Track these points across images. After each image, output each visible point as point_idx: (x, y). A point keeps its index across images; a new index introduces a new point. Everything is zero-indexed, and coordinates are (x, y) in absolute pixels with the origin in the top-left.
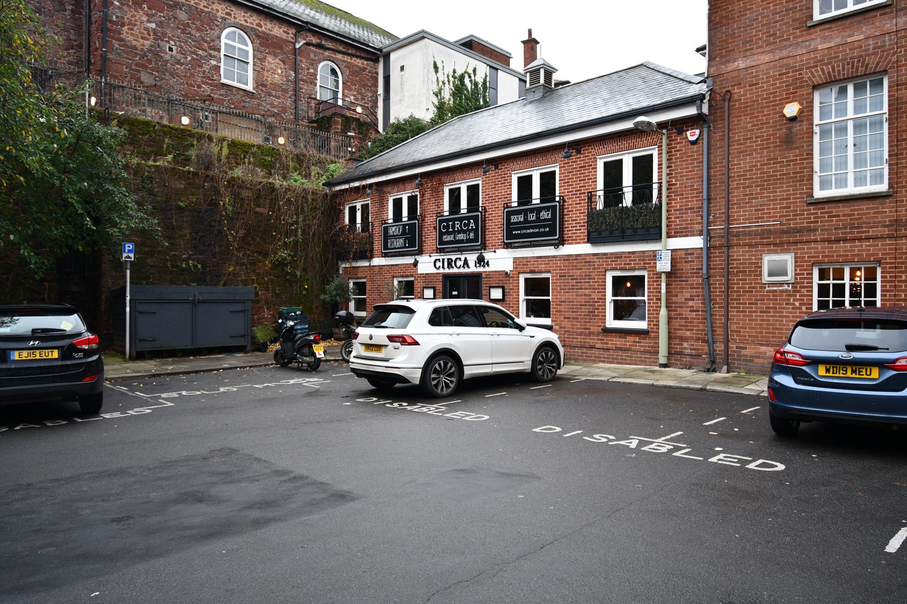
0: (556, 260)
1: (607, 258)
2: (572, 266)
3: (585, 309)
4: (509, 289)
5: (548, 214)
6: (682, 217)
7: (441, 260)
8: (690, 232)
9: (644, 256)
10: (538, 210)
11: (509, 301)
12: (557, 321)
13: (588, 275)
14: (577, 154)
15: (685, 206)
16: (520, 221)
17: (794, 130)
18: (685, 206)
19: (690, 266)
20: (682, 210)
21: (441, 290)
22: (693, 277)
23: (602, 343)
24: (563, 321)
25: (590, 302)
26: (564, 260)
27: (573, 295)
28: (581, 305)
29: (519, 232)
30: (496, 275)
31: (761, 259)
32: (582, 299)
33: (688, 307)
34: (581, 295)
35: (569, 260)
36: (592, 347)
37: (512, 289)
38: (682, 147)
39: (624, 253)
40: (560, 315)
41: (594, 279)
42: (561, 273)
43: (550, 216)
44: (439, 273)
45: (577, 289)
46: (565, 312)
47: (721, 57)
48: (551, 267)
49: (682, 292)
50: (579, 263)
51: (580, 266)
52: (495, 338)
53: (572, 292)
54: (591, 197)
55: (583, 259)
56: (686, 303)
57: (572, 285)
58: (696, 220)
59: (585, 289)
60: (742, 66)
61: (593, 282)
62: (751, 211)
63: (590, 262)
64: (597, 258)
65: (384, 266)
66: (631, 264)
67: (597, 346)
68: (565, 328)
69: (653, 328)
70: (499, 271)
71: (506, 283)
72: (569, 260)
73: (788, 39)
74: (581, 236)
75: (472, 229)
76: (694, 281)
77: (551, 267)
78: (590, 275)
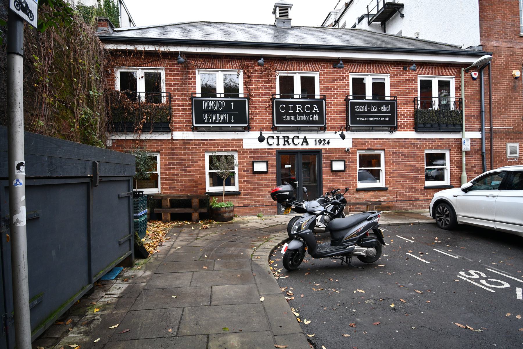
0: (389, 142)
1: (426, 141)
2: (401, 146)
3: (411, 175)
4: (349, 162)
5: (388, 108)
6: (469, 120)
7: (275, 137)
8: (473, 129)
9: (449, 141)
10: (369, 104)
11: (349, 171)
12: (391, 184)
13: (414, 153)
14: (404, 70)
15: (470, 114)
16: (364, 111)
17: (517, 83)
18: (470, 114)
19: (474, 148)
20: (469, 116)
21: (275, 163)
22: (475, 154)
23: (423, 197)
24: (395, 184)
25: (415, 170)
26: (395, 142)
27: (402, 166)
28: (408, 172)
29: (363, 119)
30: (336, 151)
31: (506, 145)
32: (409, 168)
33: (473, 171)
34: (409, 166)
35: (399, 142)
36: (417, 200)
37: (351, 162)
38: (468, 80)
39: (437, 139)
40: (393, 180)
41: (418, 155)
42: (394, 151)
43: (389, 110)
44: (273, 149)
45: (405, 162)
46: (396, 177)
47: (485, 37)
48: (385, 146)
49: (470, 163)
50: (407, 144)
51: (407, 146)
52: (491, 199)
53: (402, 164)
54: (415, 101)
55: (409, 141)
56: (472, 169)
57: (402, 159)
58: (476, 122)
59: (412, 161)
60: (495, 45)
61: (417, 157)
62: (501, 120)
63: (414, 144)
64: (419, 141)
65: (192, 140)
66: (441, 146)
67: (420, 198)
68: (397, 188)
69: (455, 185)
70: (340, 148)
71: (346, 158)
72: (399, 142)
73: (512, 39)
74: (407, 126)
75: (316, 113)
76: (476, 156)
77: (385, 146)
78: (415, 153)
